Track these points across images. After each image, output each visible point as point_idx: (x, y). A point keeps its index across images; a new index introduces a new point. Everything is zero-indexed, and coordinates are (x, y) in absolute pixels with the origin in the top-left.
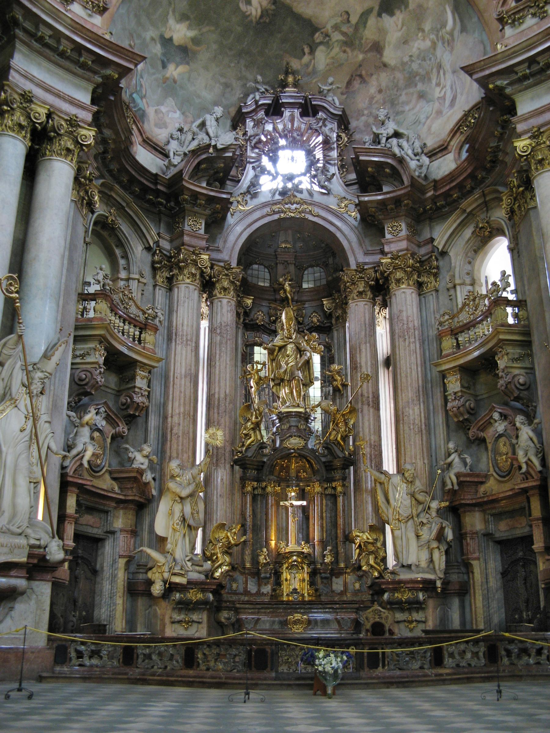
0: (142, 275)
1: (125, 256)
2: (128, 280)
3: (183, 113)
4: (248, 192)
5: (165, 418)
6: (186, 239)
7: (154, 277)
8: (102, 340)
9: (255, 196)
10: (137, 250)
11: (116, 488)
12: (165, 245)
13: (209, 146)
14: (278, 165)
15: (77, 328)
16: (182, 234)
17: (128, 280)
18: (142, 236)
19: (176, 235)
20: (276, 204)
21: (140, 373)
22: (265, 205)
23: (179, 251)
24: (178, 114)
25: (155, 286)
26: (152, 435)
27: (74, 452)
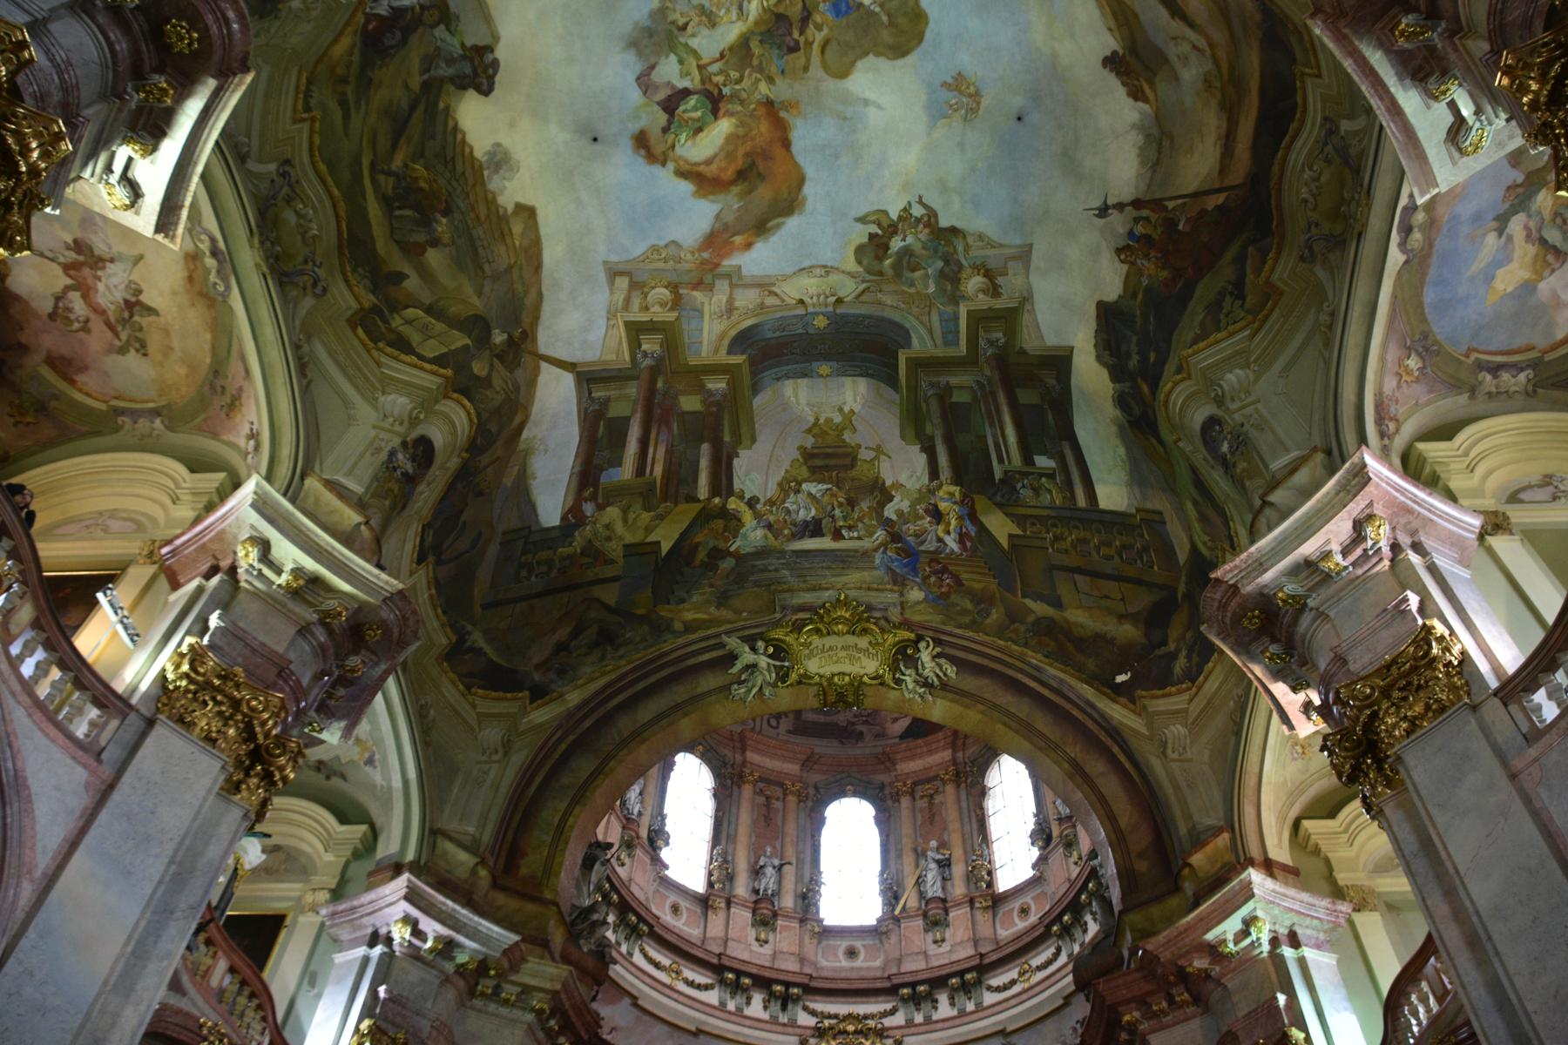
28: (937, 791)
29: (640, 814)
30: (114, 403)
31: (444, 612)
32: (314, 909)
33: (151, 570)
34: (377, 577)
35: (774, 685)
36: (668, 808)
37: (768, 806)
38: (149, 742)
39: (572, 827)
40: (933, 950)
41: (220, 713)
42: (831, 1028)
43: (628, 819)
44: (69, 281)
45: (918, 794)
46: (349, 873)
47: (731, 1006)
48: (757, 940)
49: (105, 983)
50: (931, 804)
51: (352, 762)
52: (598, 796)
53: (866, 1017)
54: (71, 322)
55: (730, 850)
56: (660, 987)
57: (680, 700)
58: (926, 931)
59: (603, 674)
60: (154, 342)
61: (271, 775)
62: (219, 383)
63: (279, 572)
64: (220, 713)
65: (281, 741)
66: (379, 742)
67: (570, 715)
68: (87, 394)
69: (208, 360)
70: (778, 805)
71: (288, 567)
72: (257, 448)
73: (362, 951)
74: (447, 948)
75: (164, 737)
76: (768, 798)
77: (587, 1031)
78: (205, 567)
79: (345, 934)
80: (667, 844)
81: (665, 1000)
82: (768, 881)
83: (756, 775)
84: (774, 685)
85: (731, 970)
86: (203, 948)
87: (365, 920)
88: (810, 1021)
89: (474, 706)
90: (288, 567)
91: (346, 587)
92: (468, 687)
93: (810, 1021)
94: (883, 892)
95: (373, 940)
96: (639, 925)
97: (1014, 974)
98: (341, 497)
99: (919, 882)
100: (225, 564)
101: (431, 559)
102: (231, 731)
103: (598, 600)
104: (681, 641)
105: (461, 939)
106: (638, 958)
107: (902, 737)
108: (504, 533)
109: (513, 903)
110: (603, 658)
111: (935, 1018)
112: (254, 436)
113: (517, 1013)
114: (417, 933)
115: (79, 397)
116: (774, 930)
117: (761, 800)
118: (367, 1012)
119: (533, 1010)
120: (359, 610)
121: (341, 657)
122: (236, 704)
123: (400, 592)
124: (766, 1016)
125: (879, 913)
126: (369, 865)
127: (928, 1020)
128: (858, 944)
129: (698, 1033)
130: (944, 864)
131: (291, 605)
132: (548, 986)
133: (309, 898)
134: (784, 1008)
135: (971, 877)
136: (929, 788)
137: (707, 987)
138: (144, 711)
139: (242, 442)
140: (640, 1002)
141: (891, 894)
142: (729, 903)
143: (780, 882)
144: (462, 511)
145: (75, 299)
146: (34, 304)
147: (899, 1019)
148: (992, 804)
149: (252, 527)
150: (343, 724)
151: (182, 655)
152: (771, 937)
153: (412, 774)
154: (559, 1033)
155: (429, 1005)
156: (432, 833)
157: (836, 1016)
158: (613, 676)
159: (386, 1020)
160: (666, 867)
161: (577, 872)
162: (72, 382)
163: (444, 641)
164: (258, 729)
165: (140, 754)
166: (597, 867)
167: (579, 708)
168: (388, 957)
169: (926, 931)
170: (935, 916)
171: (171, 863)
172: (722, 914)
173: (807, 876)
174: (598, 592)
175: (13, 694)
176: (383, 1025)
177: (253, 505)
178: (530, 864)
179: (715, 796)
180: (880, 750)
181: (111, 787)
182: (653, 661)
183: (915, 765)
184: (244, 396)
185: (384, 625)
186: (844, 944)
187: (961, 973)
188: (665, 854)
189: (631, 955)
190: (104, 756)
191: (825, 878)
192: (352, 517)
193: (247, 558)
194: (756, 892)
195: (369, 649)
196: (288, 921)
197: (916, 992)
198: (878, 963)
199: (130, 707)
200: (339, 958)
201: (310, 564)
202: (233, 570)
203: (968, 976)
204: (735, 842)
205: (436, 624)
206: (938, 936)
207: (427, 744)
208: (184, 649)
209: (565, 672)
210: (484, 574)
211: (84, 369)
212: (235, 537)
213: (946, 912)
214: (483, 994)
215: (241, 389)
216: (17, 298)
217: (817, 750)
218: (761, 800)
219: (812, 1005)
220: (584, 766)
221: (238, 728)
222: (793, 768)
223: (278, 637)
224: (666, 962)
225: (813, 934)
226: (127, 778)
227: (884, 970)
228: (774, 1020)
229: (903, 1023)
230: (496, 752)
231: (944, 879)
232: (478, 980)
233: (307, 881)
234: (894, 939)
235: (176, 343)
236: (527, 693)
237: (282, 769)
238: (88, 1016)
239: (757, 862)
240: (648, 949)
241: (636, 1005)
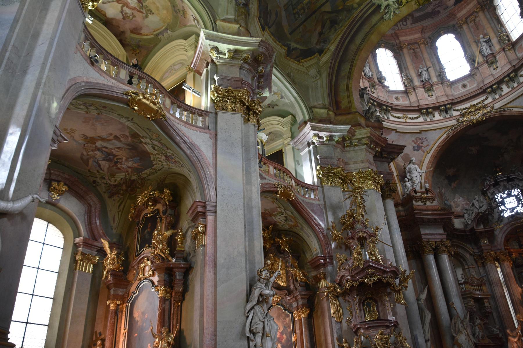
0: (472, 265)
1: (464, 260)
2: (469, 268)
3: (463, 197)
4: (498, 220)
5: (499, 313)
6: (483, 248)
7: (477, 263)
8: (471, 297)
9: (502, 221)
10: (468, 256)
11: (491, 342)
12: (476, 251)
13: (479, 213)
14: (506, 205)
15: (462, 295)
16: (481, 247)
17: (469, 268)
18: (467, 251)
19: (480, 247)
20: (511, 222)
21: (486, 301)
22: (507, 224)
23: (483, 254)
24: (461, 199)
25: (478, 267)
26: (496, 320)
27: (476, 336)
28: (476, 17)
29: (372, 75)
30: (155, 33)
31: (279, 42)
32: (288, 144)
33: (192, 73)
34: (252, 40)
35: (398, 8)
36: (380, 69)
37: (415, 52)
38: (218, 119)
39: (351, 87)
40: (494, 72)
41: (232, 102)
42: (466, 112)
43: (369, 78)
44: (121, 5)
46: (293, 131)
47: (428, 120)
48: (429, 96)
49: (243, 183)
50: (475, 23)
51: (277, 100)
52: (355, 74)
53: (477, 104)
54: (129, 17)
55: (407, 72)
56: (402, 124)
57: (367, 30)
58: (489, 67)
59: (338, 35)
60: (153, 8)
61: (256, 112)
62: (176, 9)
63: (225, 54)
64: (232, 102)
65: (253, 102)
66: (281, 90)
67: (334, 53)
68: (147, 35)
69: (170, 4)
70: (418, 50)
71: (226, 51)
72: (198, 22)
73: (307, 149)
74: (331, 138)
75: (221, 115)
76: (413, 49)
77: (384, 144)
78: (205, 65)
79: (300, 147)
80: (385, 80)
81: (406, 127)
82: (425, 76)
84: (398, 8)
85: (424, 109)
86: (264, 166)
87: (304, 141)
88: (458, 113)
89: (303, 66)
90: (226, 51)
91: (245, 48)
92: (299, 61)
93: (458, 113)
94: (468, 61)
95: (309, 145)
96: (387, 108)
98: (229, 22)
99: (481, 52)
100: (209, 60)
101: (266, 27)
102: (238, 105)
103: (325, 12)
104: (359, 10)
105: (333, 134)
106: (391, 118)
107: (455, 4)
108: (284, 7)
109: (344, 117)
110: (336, 30)
111: (503, 94)
112: (195, 19)
113: (360, 147)
114: (320, 137)
115: (145, 37)
116: (433, 91)
117: (411, 51)
118: (317, 164)
119: (364, 144)
120: (253, 53)
121: (256, 70)
122: (235, 97)
123: (262, 41)
124: (442, 118)
125: (469, 69)
126: (297, 126)
127: (501, 96)
128: (465, 82)
129: (421, 132)
130: (488, 41)
131: (233, 62)
132: (366, 136)
133: (286, 142)
134: (447, 113)
135: (501, 41)
136: (472, 17)
137: (418, 117)
138: (212, 111)
139: (193, 23)
141: (471, 60)
142: (414, 89)
143: (429, 75)
144: (267, 8)
145: (125, 8)
146: (117, 18)
147: (490, 100)
149: (210, 45)
150: (267, 89)
151: (213, 92)
153: (296, 95)
154: (376, 147)
155: (333, 155)
156: (310, 109)
157: (466, 108)
158: (342, 34)
159: (323, 164)
160: (388, 87)
161: (359, 100)
162: (141, 34)
163: (284, 51)
164: (245, 101)
165: (218, 123)
166: (365, 96)
167: (336, 50)
168: (315, 148)
169: (489, 67)
170: (491, 61)
171: (242, 147)
172: (413, 93)
173: (438, 68)
174: (324, 9)
175: (178, 123)
176: (323, 166)
177: (206, 39)
178: (344, 104)
179: (395, 57)
180: (448, 13)
181: (216, 135)
182: (352, 22)
183: (464, 12)
184: (185, 8)
185: (262, 53)
186: (460, 85)
187: (508, 75)
188: (386, 83)
189: (389, 118)
190: (210, 128)
191: (445, 66)
192: (236, 26)
193: (214, 55)
194: (422, 81)
195: (262, 63)
196: (283, 151)
197: (494, 88)
198: (475, 85)
199: (208, 112)
200: (302, 154)
201: (232, 47)
202: (212, 61)
203: (511, 75)
204: (408, 69)
205: (279, 47)
206: (495, 67)
207: (295, 84)
208: (213, 89)
209: (326, 41)
210: (285, 23)
211: (141, 28)
212: (207, 51)
213: (495, 57)
214: (347, 146)
215: (183, 7)
216: (112, 19)
217: (424, 25)
218: (411, 51)
219: (456, 108)
220: (346, 67)
221: (239, 104)
222: (418, 35)
223: (235, 73)
224: (401, 115)
225: (448, 86)
226: (219, 131)
227: (478, 87)
228: (445, 118)
229: (492, 100)
230: (317, 76)
231: (490, 46)
232: (344, 143)
233: (283, 138)
234: (478, 75)
235: (158, 5)
236: (317, 54)
237: (257, 109)
238: (244, 193)
239: (418, 72)
240: (393, 114)
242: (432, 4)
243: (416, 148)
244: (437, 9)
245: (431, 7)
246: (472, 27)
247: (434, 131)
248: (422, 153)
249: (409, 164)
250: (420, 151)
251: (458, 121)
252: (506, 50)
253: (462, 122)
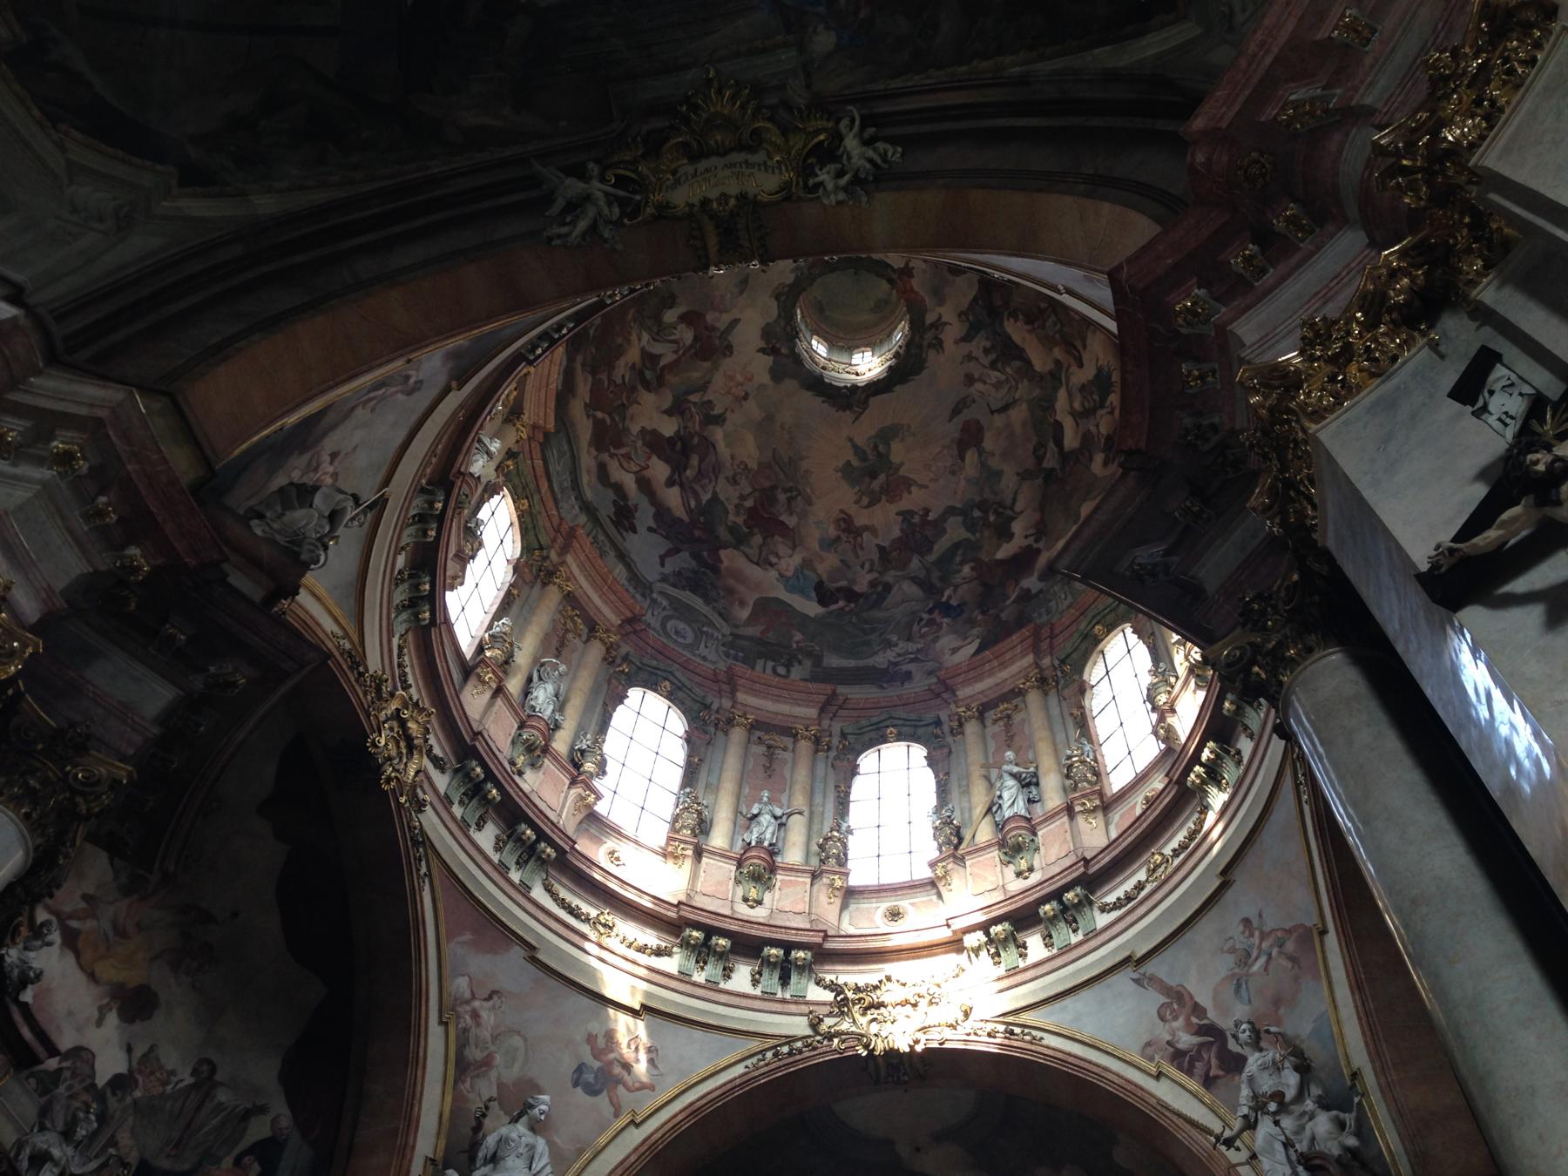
35: (618, 224)
45: (988, 722)
48: (746, 900)
50: (1008, 726)
76: (769, 747)
83: (751, 717)
84: (618, 224)
85: (697, 926)
88: (829, 996)
97: (1142, 875)
106: (538, 893)
113: (25, 470)
117: (761, 749)
124: (758, 992)
134: (785, 981)
140: (541, 956)
142: (699, 853)
148: (1096, 701)
152: (767, 897)
203: (1069, 896)
218: (761, 749)
240: (557, 887)
241: (534, 960)
242: (897, 649)
243: (590, 1077)
244: (905, 668)
245: (890, 655)
246: (993, 737)
247: (698, 1034)
248: (608, 1110)
249: (515, 1120)
250: (603, 1100)
251: (814, 1026)
252: (1078, 808)
253: (830, 1037)
